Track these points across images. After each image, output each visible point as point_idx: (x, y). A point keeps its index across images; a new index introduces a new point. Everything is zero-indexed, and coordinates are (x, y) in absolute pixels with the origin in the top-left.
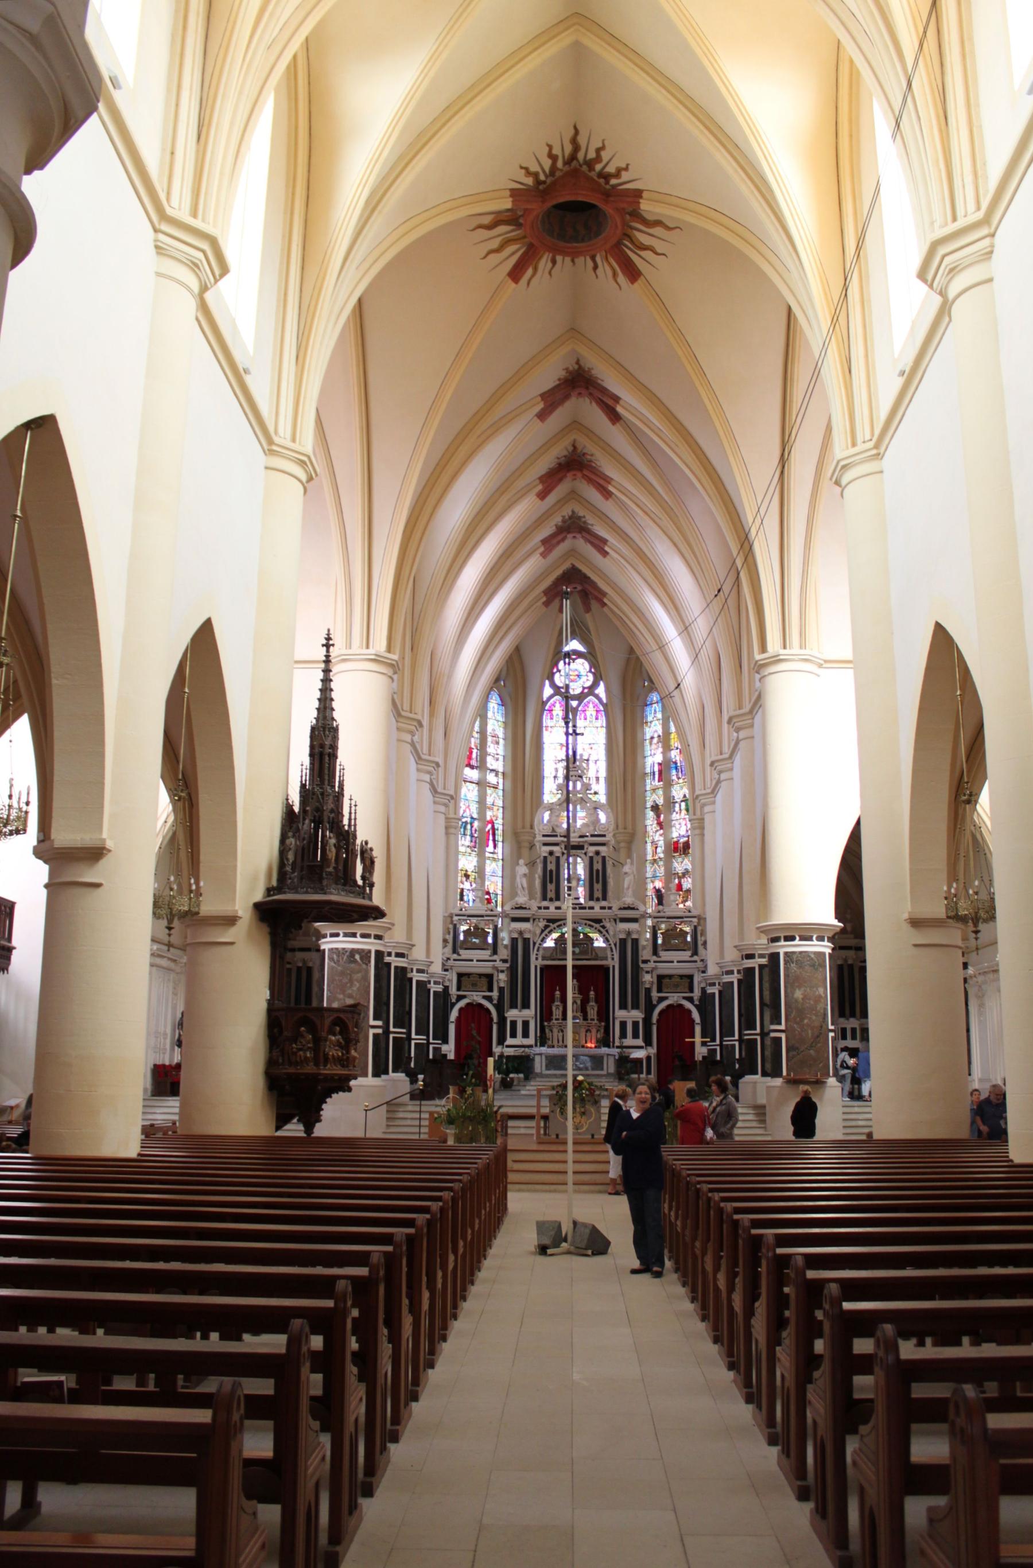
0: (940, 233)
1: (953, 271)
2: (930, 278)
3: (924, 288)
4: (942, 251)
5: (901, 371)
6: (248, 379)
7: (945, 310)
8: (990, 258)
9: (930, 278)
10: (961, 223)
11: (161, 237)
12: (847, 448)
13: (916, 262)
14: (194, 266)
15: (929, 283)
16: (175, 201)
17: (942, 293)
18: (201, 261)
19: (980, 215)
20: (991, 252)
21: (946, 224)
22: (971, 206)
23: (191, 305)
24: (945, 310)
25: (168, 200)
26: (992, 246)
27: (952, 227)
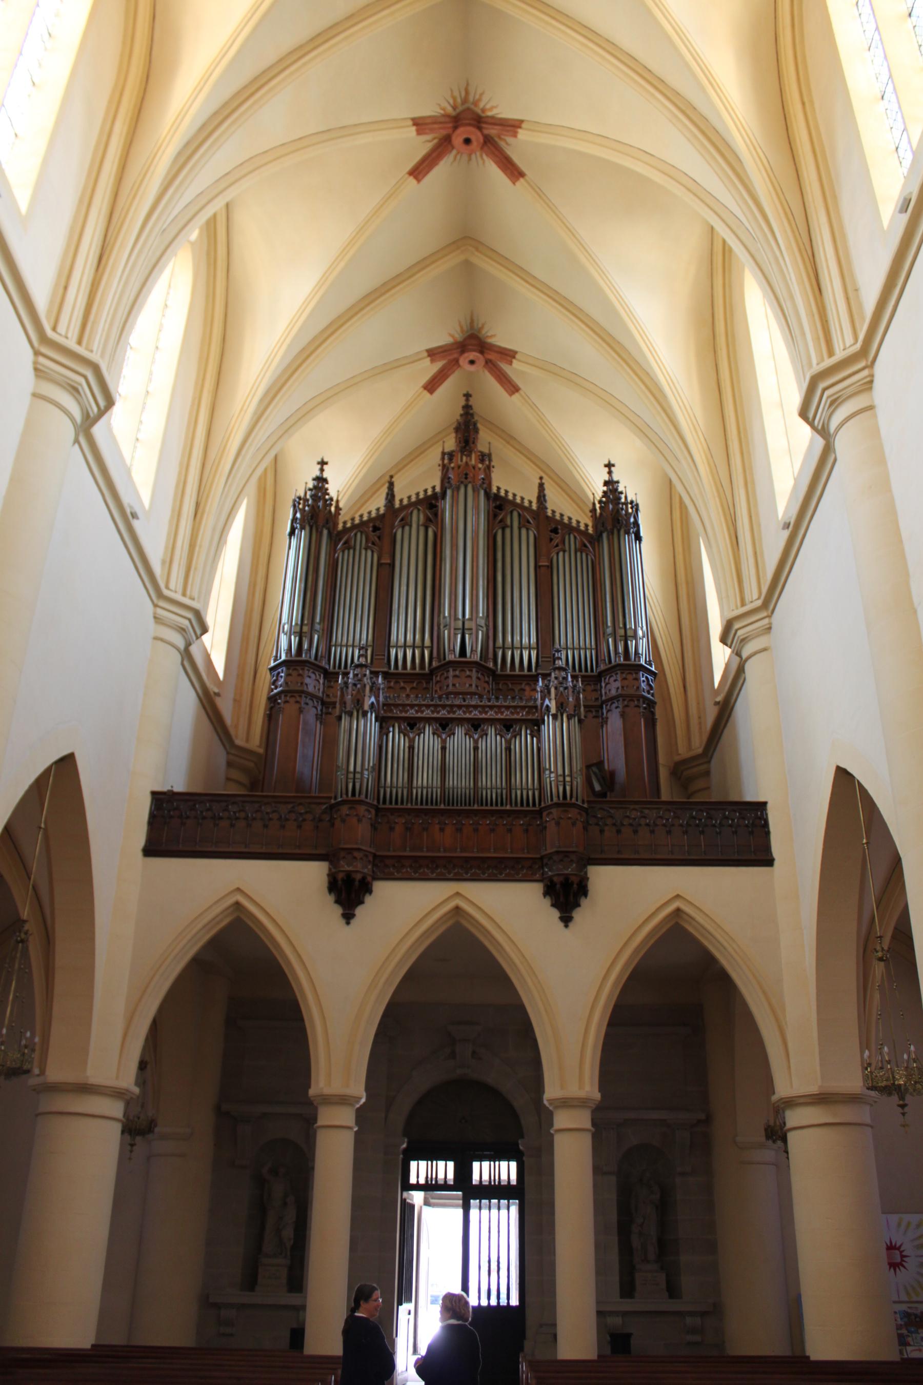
0: (816, 368)
1: (835, 403)
2: (811, 415)
3: (806, 429)
4: (822, 385)
5: (785, 523)
6: (136, 524)
7: (828, 450)
8: (870, 389)
9: (811, 415)
10: (840, 355)
11: (41, 360)
12: (737, 608)
13: (795, 399)
14: (74, 390)
15: (810, 420)
16: (62, 328)
17: (823, 432)
18: (81, 385)
19: (858, 346)
20: (871, 382)
21: (822, 360)
22: (849, 340)
23: (68, 431)
24: (828, 450)
25: (54, 329)
26: (872, 376)
27: (828, 362)
